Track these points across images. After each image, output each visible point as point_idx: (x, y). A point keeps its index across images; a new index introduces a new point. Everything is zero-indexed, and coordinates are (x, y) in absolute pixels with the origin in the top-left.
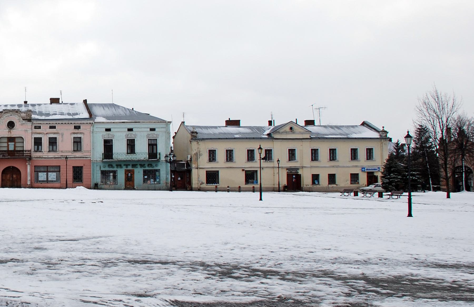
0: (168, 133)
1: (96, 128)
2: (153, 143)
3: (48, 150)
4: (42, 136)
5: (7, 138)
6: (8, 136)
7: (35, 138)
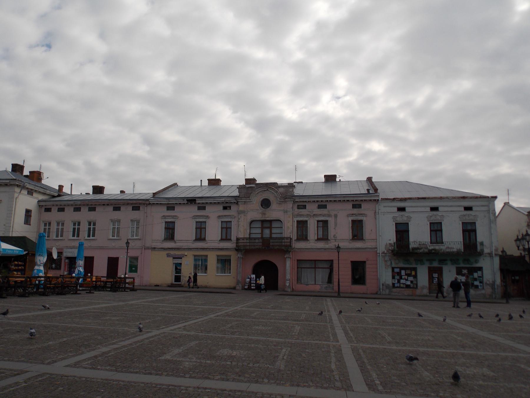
0: (492, 213)
1: (384, 207)
2: (469, 228)
3: (316, 238)
4: (308, 218)
5: (260, 222)
6: (262, 219)
7: (297, 221)
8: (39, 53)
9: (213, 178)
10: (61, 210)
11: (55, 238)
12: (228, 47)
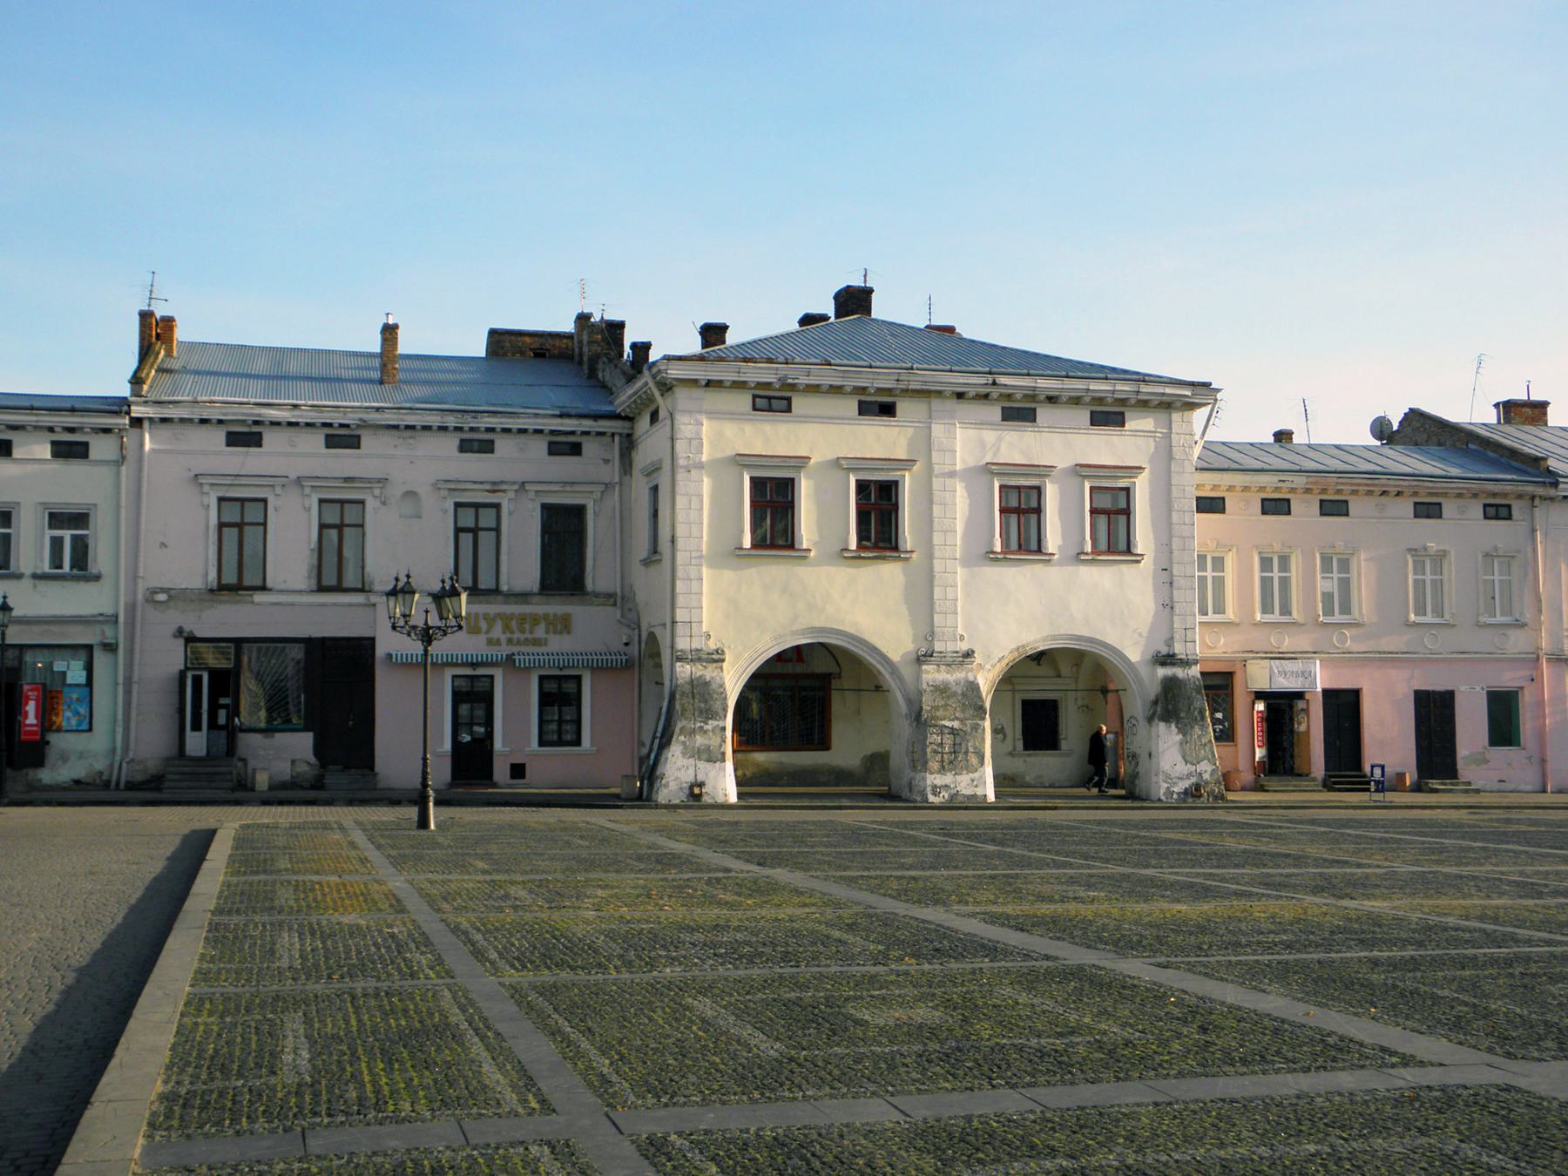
9: (1521, 396)
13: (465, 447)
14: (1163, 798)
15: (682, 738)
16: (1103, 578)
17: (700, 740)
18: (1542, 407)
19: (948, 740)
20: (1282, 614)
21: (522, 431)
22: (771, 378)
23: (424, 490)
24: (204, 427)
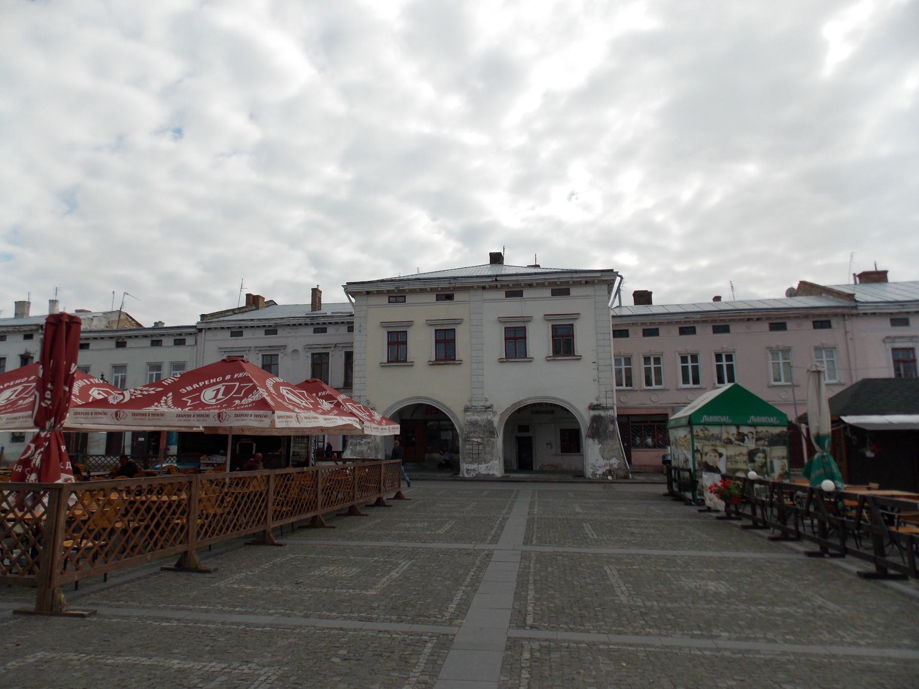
8: (167, 143)
10: (651, 332)
11: (644, 387)
12: (427, 129)
13: (316, 331)
14: (591, 477)
15: (351, 447)
16: (564, 368)
17: (358, 448)
18: (884, 273)
19: (475, 447)
20: (694, 384)
21: (336, 323)
22: (393, 288)
23: (300, 348)
24: (223, 330)
